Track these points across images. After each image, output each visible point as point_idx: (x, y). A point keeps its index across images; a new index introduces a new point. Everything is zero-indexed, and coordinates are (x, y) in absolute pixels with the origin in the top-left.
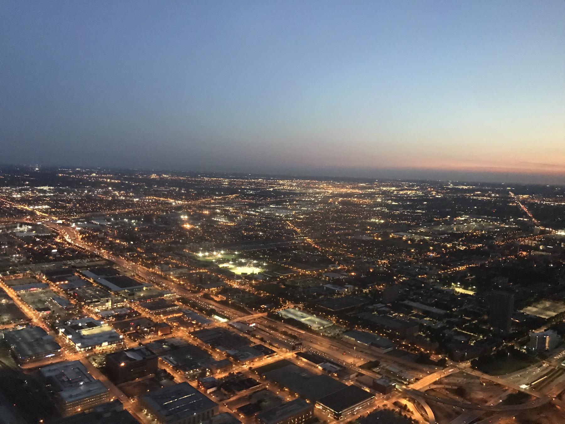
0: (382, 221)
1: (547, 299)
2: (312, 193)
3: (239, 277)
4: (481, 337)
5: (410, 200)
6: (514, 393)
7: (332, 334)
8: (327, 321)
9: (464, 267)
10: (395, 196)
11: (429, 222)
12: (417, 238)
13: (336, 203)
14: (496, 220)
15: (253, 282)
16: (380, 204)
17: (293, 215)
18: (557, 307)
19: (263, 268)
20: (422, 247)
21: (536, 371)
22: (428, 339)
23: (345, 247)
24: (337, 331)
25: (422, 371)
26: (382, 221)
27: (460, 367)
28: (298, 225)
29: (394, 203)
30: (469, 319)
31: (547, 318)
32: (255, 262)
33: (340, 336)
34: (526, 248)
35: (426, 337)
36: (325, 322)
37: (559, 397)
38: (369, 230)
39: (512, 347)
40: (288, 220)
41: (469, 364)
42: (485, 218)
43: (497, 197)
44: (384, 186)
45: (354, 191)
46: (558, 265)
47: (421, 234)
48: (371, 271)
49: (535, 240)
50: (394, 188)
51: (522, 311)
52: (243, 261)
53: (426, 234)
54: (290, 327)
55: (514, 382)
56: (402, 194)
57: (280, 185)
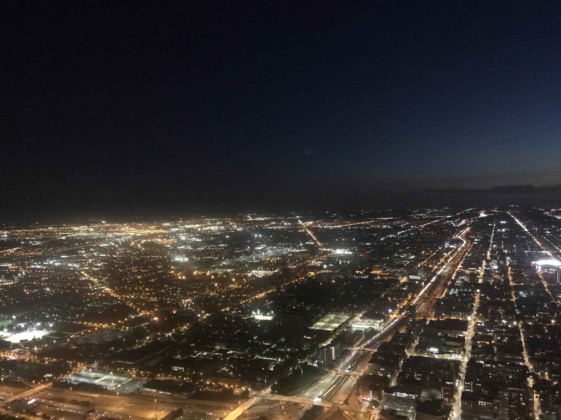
0: (187, 259)
1: (332, 312)
2: (112, 238)
3: (16, 346)
4: (280, 360)
5: (214, 236)
6: (309, 408)
7: (132, 390)
8: (125, 376)
9: (263, 294)
10: (199, 233)
11: (230, 255)
12: (220, 272)
13: (139, 246)
14: (289, 246)
15: (36, 349)
16: (185, 243)
17: (89, 263)
18: (340, 319)
19: (49, 330)
20: (224, 280)
21: (327, 381)
22: (231, 373)
23: (147, 292)
24: (138, 385)
25: (226, 409)
26: (187, 259)
27: (262, 395)
28: (94, 274)
29: (198, 240)
30: (269, 344)
31: (332, 330)
32: (39, 324)
33: (141, 390)
34: (313, 268)
35: (229, 371)
36: (123, 379)
37: (346, 402)
38: (173, 270)
39: (306, 363)
40: (82, 270)
41: (270, 389)
42: (279, 246)
43: (289, 226)
44: (188, 224)
45: (157, 231)
46: (337, 280)
47: (224, 267)
48: (174, 312)
49: (320, 260)
50: (197, 226)
51: (312, 328)
52: (22, 325)
53: (228, 267)
54: (81, 394)
55: (308, 397)
56: (205, 231)
57: (75, 232)
